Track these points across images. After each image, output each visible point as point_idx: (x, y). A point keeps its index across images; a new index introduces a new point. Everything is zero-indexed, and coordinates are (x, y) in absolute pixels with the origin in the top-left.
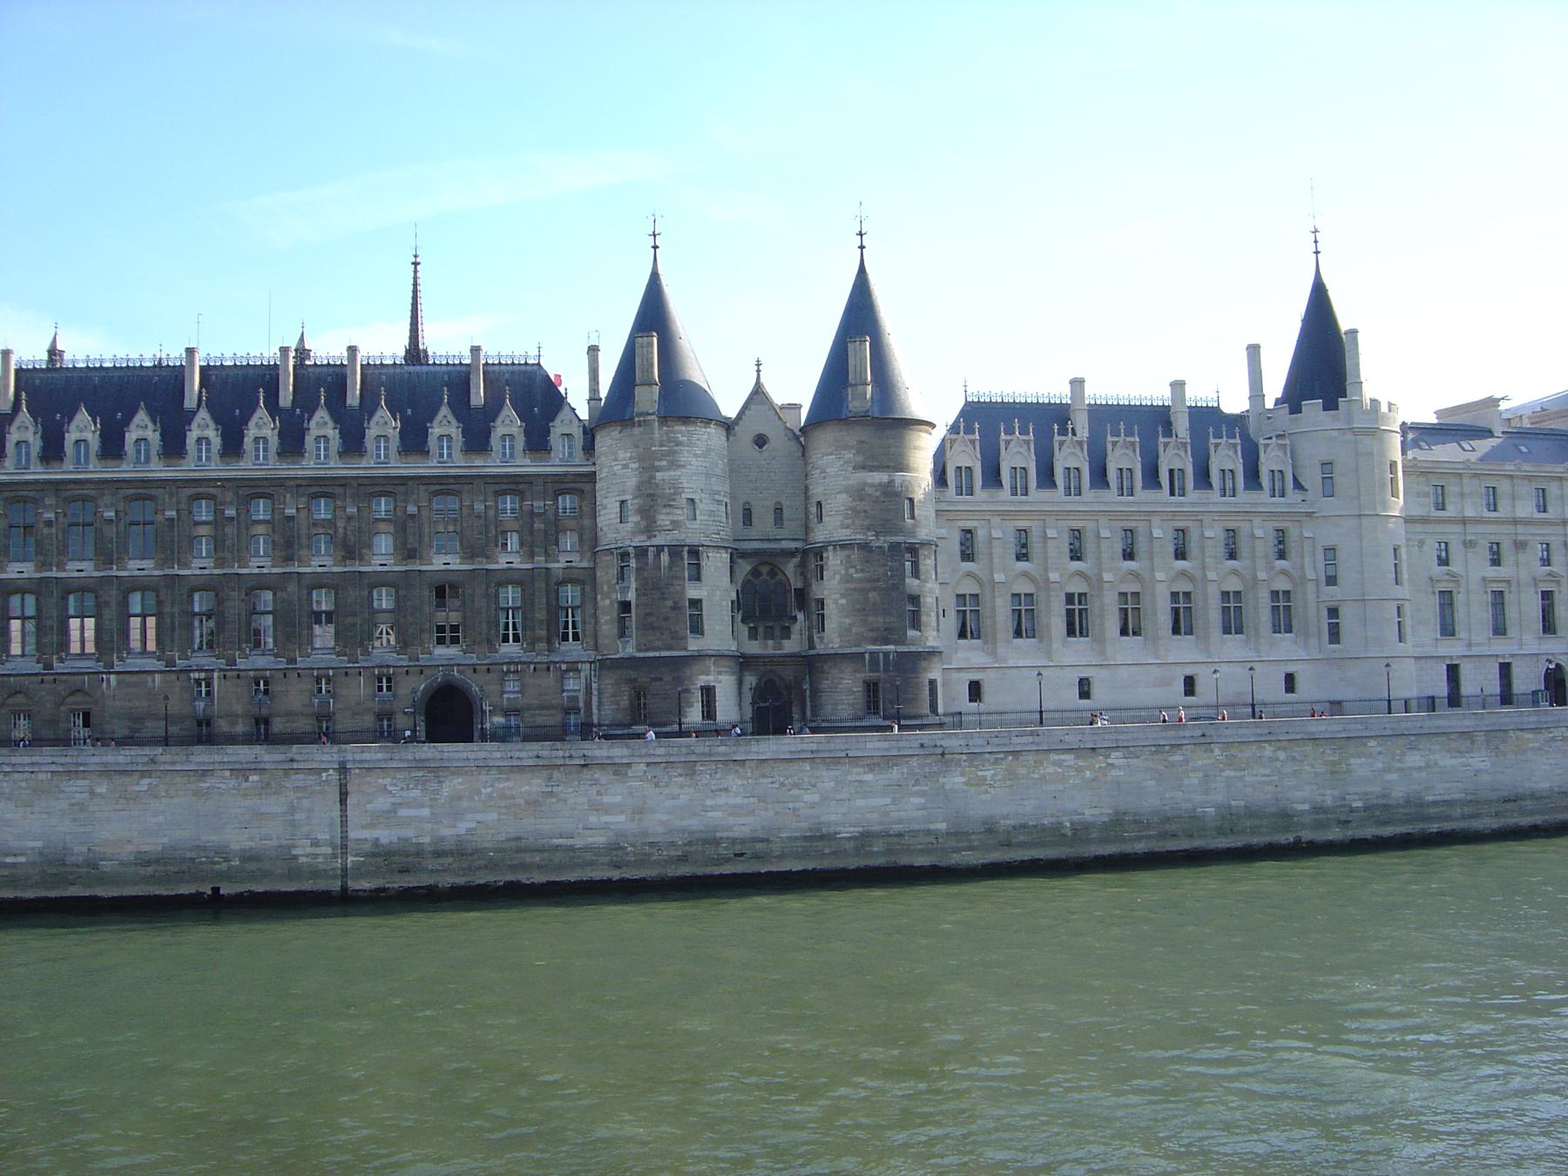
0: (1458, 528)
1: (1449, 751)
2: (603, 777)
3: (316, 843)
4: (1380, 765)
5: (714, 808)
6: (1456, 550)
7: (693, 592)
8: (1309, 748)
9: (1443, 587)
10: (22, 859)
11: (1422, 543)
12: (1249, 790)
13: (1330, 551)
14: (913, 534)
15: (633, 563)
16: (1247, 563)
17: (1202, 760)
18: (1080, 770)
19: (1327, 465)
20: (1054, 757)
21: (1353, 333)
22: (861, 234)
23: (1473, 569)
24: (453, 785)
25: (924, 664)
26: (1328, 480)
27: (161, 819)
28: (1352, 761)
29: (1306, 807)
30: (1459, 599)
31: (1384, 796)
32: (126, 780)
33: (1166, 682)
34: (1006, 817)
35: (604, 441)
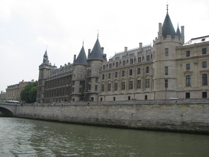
1: (127, 108)
4: (114, 111)
6: (192, 65)
7: (73, 87)
8: (103, 106)
9: (187, 74)
11: (181, 66)
12: (93, 114)
14: (90, 76)
16: (141, 74)
17: (88, 107)
18: (74, 108)
20: (72, 106)
22: (98, 35)
25: (90, 95)
28: (109, 109)
29: (101, 118)
30: (191, 77)
31: (114, 117)
33: (125, 98)
34: (66, 115)
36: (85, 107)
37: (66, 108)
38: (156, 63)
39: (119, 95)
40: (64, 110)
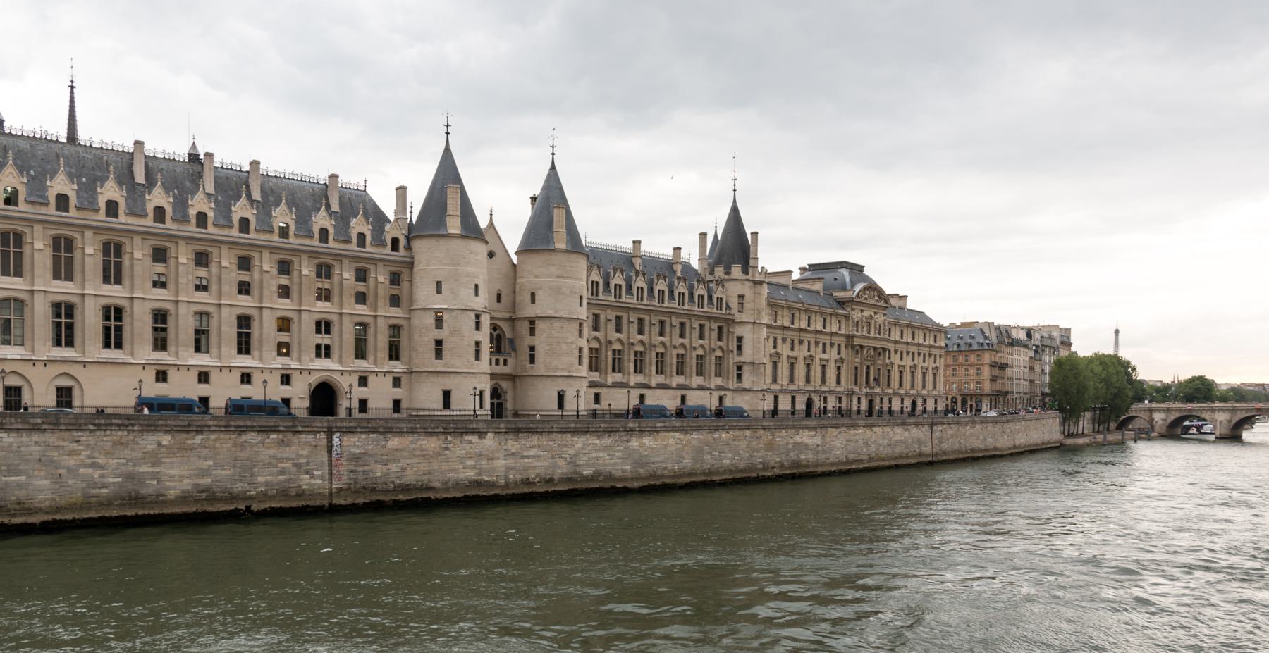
0: (779, 332)
2: (474, 439)
3: (313, 476)
5: (528, 457)
6: (779, 341)
10: (105, 491)
13: (740, 339)
15: (446, 316)
21: (755, 234)
23: (785, 350)
24: (395, 442)
26: (741, 304)
27: (211, 463)
32: (184, 436)
33: (675, 398)
35: (417, 244)
36: (716, 436)
37: (648, 441)
38: (750, 326)
39: (659, 392)
40: (642, 445)
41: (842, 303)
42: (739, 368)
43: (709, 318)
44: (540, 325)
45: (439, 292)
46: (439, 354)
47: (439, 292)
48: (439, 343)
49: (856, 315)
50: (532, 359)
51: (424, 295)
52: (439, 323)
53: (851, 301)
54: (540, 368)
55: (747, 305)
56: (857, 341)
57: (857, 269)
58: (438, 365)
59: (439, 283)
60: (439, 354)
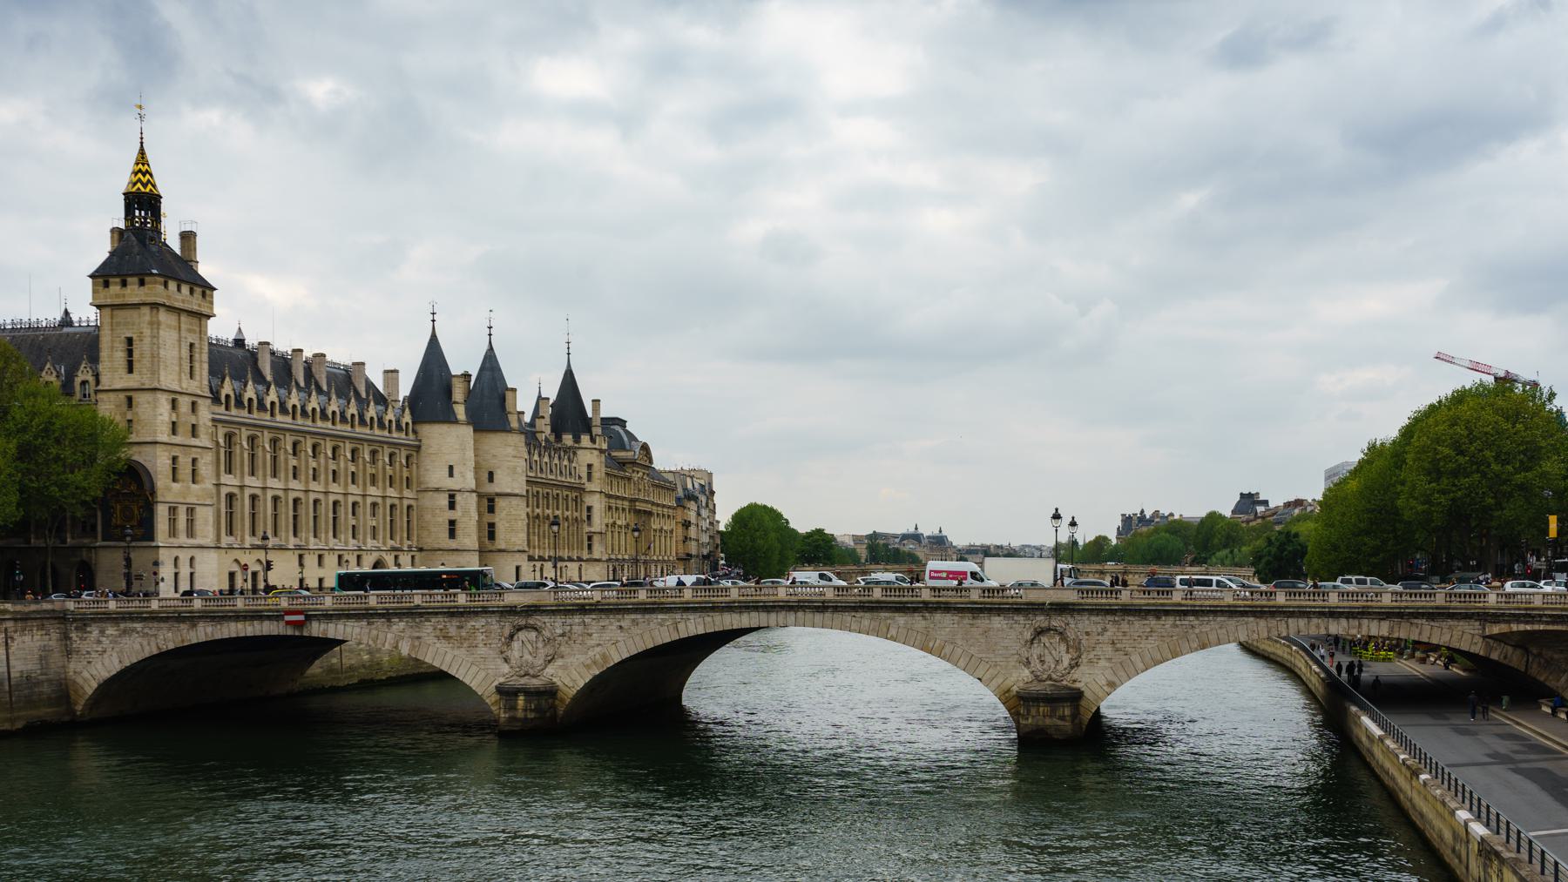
13: (589, 509)
15: (458, 498)
19: (590, 466)
41: (622, 464)
42: (590, 539)
43: (571, 488)
44: (501, 503)
45: (451, 475)
46: (452, 534)
47: (451, 475)
48: (452, 523)
49: (636, 476)
50: (492, 536)
51: (436, 476)
52: (452, 506)
53: (633, 463)
54: (500, 543)
55: (596, 475)
56: (640, 506)
57: (622, 423)
58: (453, 544)
59: (451, 468)
60: (452, 534)
